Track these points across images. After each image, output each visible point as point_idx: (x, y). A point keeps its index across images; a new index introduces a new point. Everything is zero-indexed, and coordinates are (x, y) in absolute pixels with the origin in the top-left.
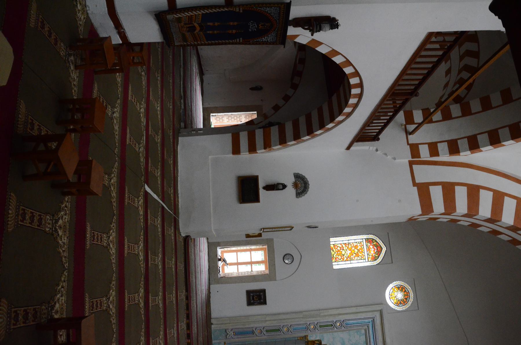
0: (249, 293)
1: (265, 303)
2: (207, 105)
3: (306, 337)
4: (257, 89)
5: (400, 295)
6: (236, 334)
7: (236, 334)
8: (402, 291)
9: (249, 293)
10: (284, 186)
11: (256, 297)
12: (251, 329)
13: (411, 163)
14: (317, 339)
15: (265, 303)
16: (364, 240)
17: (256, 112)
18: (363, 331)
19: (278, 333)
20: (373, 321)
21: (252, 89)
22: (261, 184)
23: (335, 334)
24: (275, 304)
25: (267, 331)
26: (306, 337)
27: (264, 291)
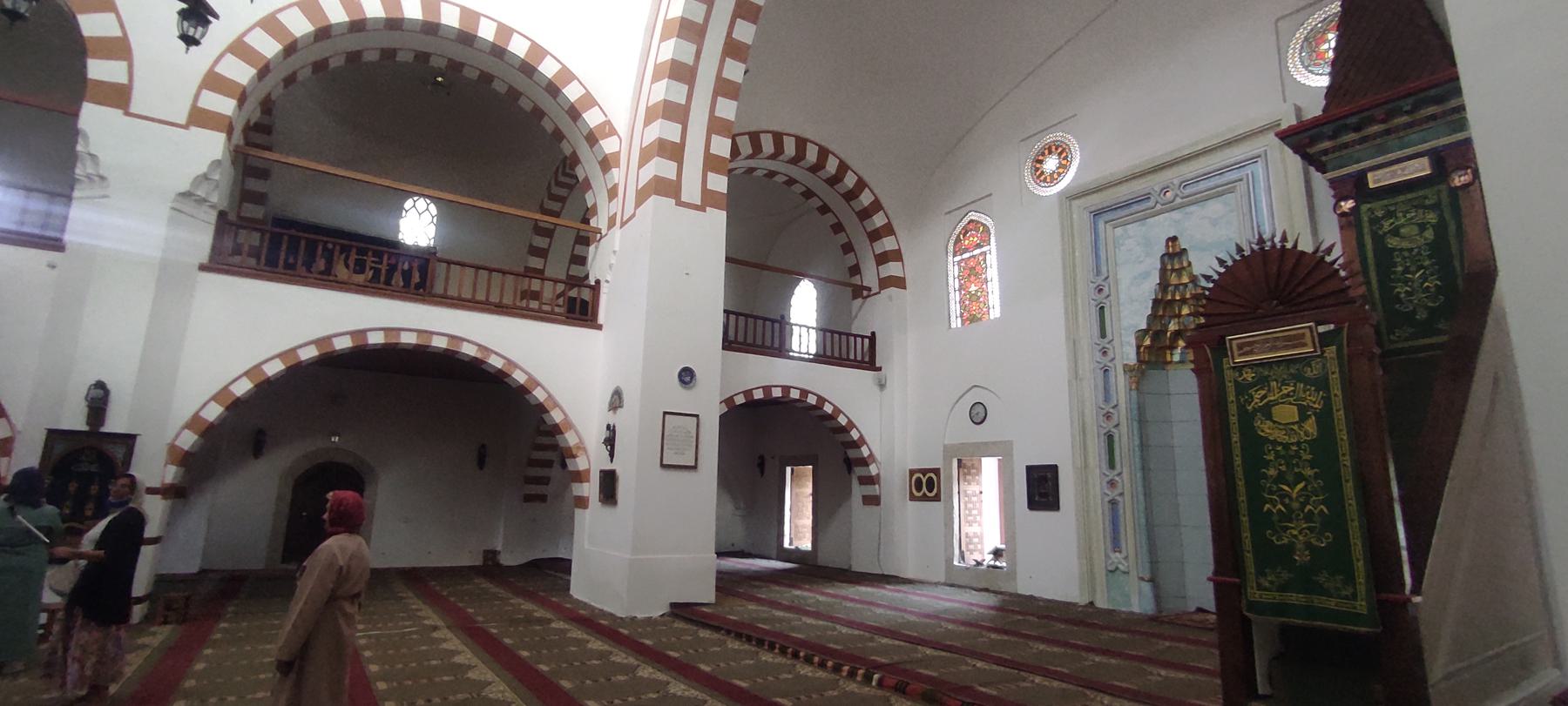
0: (1033, 505)
1: (1054, 469)
2: (774, 553)
3: (1128, 369)
4: (761, 465)
5: (1051, 164)
6: (1116, 545)
7: (1116, 545)
8: (1041, 162)
9: (1033, 505)
10: (611, 429)
11: (1042, 488)
12: (1107, 506)
13: (623, 224)
14: (1133, 342)
15: (1054, 469)
16: (958, 258)
17: (789, 469)
18: (1119, 231)
19: (1116, 438)
20: (1097, 214)
21: (762, 473)
22: (609, 467)
23: (1123, 297)
24: (1055, 449)
25: (1112, 466)
26: (1128, 369)
27: (1030, 469)
